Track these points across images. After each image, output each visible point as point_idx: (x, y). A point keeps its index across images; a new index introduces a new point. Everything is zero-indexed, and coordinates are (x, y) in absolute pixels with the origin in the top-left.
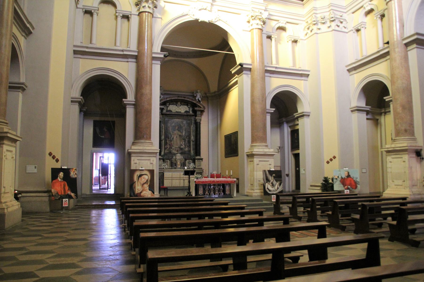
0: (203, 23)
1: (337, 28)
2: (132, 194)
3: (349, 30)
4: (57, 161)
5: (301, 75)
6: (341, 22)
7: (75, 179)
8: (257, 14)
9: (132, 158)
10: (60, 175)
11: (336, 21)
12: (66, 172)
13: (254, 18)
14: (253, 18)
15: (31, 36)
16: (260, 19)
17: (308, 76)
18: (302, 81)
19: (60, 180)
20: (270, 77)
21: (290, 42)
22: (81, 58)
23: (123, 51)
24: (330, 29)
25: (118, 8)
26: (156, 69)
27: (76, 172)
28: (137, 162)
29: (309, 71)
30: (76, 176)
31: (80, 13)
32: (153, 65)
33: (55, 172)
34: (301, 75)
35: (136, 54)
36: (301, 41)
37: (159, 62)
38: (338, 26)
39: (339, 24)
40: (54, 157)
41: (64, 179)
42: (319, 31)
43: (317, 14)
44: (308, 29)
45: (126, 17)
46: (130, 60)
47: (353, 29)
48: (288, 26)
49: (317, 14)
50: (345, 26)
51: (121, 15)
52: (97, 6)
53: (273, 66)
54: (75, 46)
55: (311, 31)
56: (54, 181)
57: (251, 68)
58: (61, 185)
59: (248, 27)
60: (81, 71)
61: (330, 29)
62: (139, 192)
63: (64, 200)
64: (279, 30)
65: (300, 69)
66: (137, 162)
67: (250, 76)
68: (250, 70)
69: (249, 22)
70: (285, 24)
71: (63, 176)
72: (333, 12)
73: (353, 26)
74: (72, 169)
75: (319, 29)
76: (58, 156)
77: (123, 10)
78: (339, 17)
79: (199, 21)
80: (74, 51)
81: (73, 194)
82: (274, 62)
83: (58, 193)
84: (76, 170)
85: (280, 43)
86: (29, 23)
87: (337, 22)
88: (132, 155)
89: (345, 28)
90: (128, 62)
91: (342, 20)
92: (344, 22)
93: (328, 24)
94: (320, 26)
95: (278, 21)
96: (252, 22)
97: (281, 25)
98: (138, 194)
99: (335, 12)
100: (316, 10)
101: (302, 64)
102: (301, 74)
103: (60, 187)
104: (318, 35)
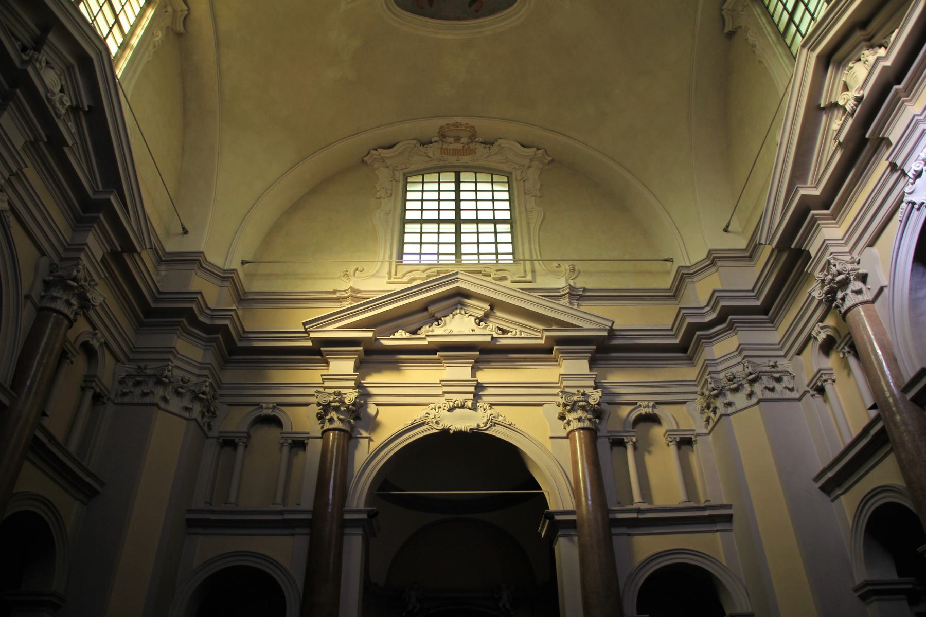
0: (460, 434)
1: (769, 395)
3: (801, 392)
5: (712, 520)
6: (779, 380)
8: (576, 398)
11: (765, 378)
13: (573, 407)
14: (568, 408)
16: (583, 408)
17: (728, 518)
18: (718, 533)
20: (629, 535)
21: (673, 448)
22: (200, 534)
23: (281, 512)
24: (754, 400)
25: (286, 429)
26: (354, 545)
29: (729, 506)
32: (345, 538)
34: (712, 520)
35: (309, 516)
36: (698, 438)
37: (360, 531)
38: (772, 390)
39: (772, 384)
42: (730, 410)
43: (718, 372)
44: (708, 407)
45: (299, 444)
46: (298, 530)
47: (808, 389)
48: (661, 411)
49: (718, 372)
50: (790, 386)
51: (290, 441)
52: (245, 430)
53: (635, 506)
54: (190, 511)
55: (715, 413)
57: (575, 521)
59: (560, 429)
61: (754, 400)
64: (641, 426)
65: (707, 504)
67: (576, 539)
68: (572, 524)
69: (562, 417)
70: (654, 407)
72: (748, 362)
73: (806, 382)
75: (729, 404)
77: (294, 430)
78: (768, 369)
79: (451, 432)
82: (637, 497)
85: (650, 452)
86: (90, 474)
87: (766, 381)
89: (791, 390)
90: (293, 535)
91: (777, 375)
92: (785, 378)
93: (747, 389)
94: (730, 397)
95: (636, 403)
96: (570, 416)
97: (643, 411)
99: (750, 359)
100: (715, 365)
101: (713, 492)
102: (710, 516)
104: (731, 417)
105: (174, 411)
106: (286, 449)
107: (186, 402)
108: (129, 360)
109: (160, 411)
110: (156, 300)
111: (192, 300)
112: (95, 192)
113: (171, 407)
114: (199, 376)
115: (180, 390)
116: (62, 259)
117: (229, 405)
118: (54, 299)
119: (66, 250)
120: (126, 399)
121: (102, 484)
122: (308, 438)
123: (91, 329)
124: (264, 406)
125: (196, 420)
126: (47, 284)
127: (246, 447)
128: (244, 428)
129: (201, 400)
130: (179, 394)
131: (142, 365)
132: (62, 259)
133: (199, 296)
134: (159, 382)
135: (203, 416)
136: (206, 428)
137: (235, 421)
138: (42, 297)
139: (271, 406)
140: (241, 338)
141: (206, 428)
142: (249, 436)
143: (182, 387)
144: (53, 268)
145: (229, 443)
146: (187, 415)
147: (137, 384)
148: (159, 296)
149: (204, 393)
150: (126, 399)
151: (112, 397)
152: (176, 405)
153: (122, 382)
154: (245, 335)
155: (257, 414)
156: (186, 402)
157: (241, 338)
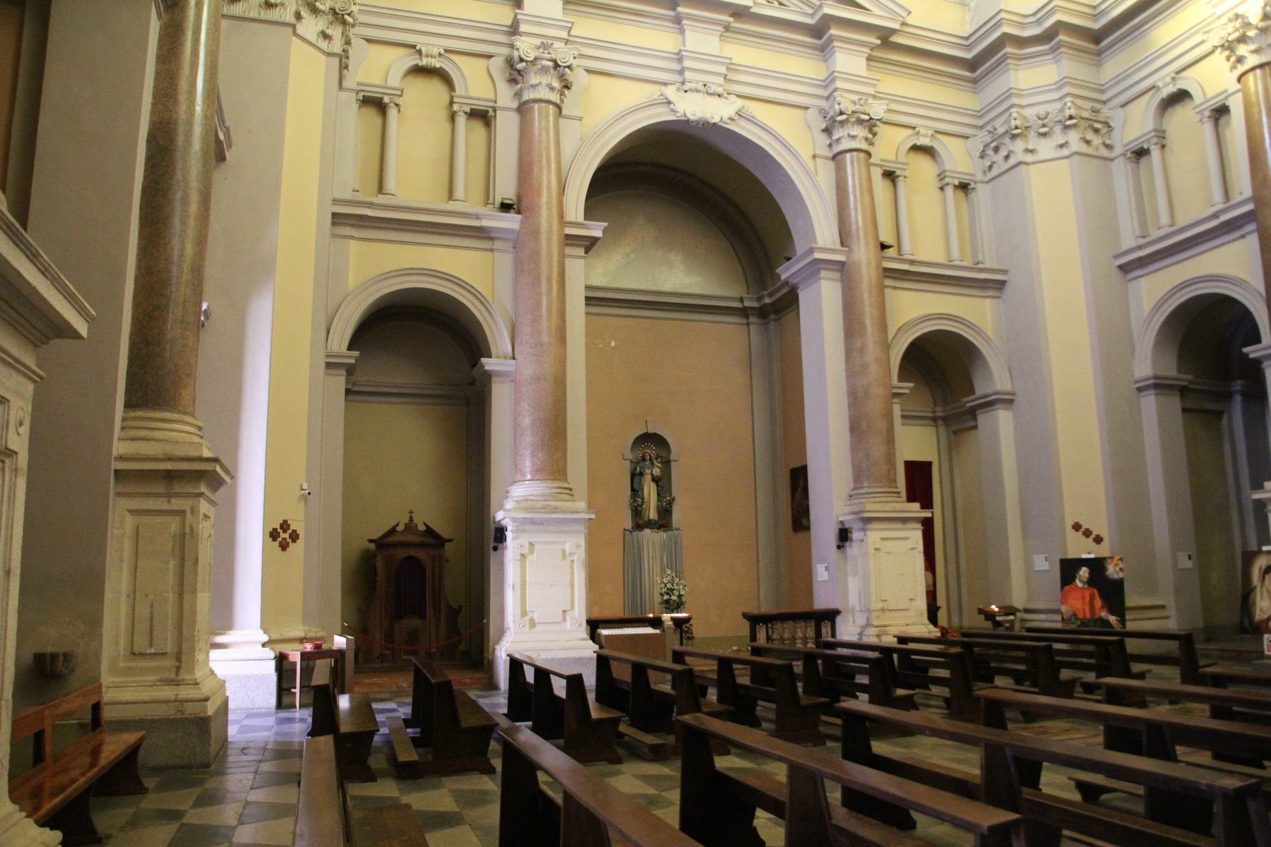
2: (1247, 623)
4: (1098, 540)
7: (1120, 583)
12: (1097, 566)
15: (1008, 287)
19: (1080, 585)
23: (1215, 216)
25: (1198, 97)
27: (1121, 565)
30: (1121, 575)
31: (1121, 170)
33: (1069, 568)
35: (1250, 207)
40: (1087, 533)
41: (1091, 582)
45: (1221, 112)
51: (1207, 113)
56: (1067, 588)
58: (1083, 598)
60: (1147, 308)
62: (1265, 616)
76: (1100, 528)
77: (1209, 95)
80: (1121, 267)
81: (1112, 619)
83: (1075, 615)
84: (1121, 559)
90: (1243, 236)
98: (1261, 622)
103: (1083, 601)
105: (1048, 157)
106: (1208, 127)
107: (1059, 137)
108: (981, 128)
109: (1031, 167)
110: (968, 48)
111: (998, 24)
112: (812, 15)
113: (1042, 155)
114: (1060, 99)
115: (1043, 130)
116: (827, 98)
117: (1122, 106)
118: (838, 140)
119: (825, 87)
120: (995, 172)
121: (1005, 272)
122: (1227, 98)
123: (910, 132)
124: (1160, 84)
126: (827, 131)
127: (1163, 146)
128: (1150, 126)
129: (1074, 126)
130: (1044, 135)
131: (990, 128)
132: (827, 98)
133: (1003, 15)
134: (1014, 137)
135: (1088, 142)
136: (1104, 152)
137: (1136, 123)
138: (830, 146)
139: (1168, 79)
140: (1095, 17)
141: (1104, 152)
142: (1161, 135)
143: (1044, 126)
144: (823, 113)
145: (1141, 153)
146: (1065, 152)
147: (996, 149)
148: (966, 42)
149: (1071, 117)
150: (995, 172)
151: (979, 177)
152: (1046, 148)
153: (982, 157)
154: (1098, 10)
156: (1059, 137)
157: (1095, 17)
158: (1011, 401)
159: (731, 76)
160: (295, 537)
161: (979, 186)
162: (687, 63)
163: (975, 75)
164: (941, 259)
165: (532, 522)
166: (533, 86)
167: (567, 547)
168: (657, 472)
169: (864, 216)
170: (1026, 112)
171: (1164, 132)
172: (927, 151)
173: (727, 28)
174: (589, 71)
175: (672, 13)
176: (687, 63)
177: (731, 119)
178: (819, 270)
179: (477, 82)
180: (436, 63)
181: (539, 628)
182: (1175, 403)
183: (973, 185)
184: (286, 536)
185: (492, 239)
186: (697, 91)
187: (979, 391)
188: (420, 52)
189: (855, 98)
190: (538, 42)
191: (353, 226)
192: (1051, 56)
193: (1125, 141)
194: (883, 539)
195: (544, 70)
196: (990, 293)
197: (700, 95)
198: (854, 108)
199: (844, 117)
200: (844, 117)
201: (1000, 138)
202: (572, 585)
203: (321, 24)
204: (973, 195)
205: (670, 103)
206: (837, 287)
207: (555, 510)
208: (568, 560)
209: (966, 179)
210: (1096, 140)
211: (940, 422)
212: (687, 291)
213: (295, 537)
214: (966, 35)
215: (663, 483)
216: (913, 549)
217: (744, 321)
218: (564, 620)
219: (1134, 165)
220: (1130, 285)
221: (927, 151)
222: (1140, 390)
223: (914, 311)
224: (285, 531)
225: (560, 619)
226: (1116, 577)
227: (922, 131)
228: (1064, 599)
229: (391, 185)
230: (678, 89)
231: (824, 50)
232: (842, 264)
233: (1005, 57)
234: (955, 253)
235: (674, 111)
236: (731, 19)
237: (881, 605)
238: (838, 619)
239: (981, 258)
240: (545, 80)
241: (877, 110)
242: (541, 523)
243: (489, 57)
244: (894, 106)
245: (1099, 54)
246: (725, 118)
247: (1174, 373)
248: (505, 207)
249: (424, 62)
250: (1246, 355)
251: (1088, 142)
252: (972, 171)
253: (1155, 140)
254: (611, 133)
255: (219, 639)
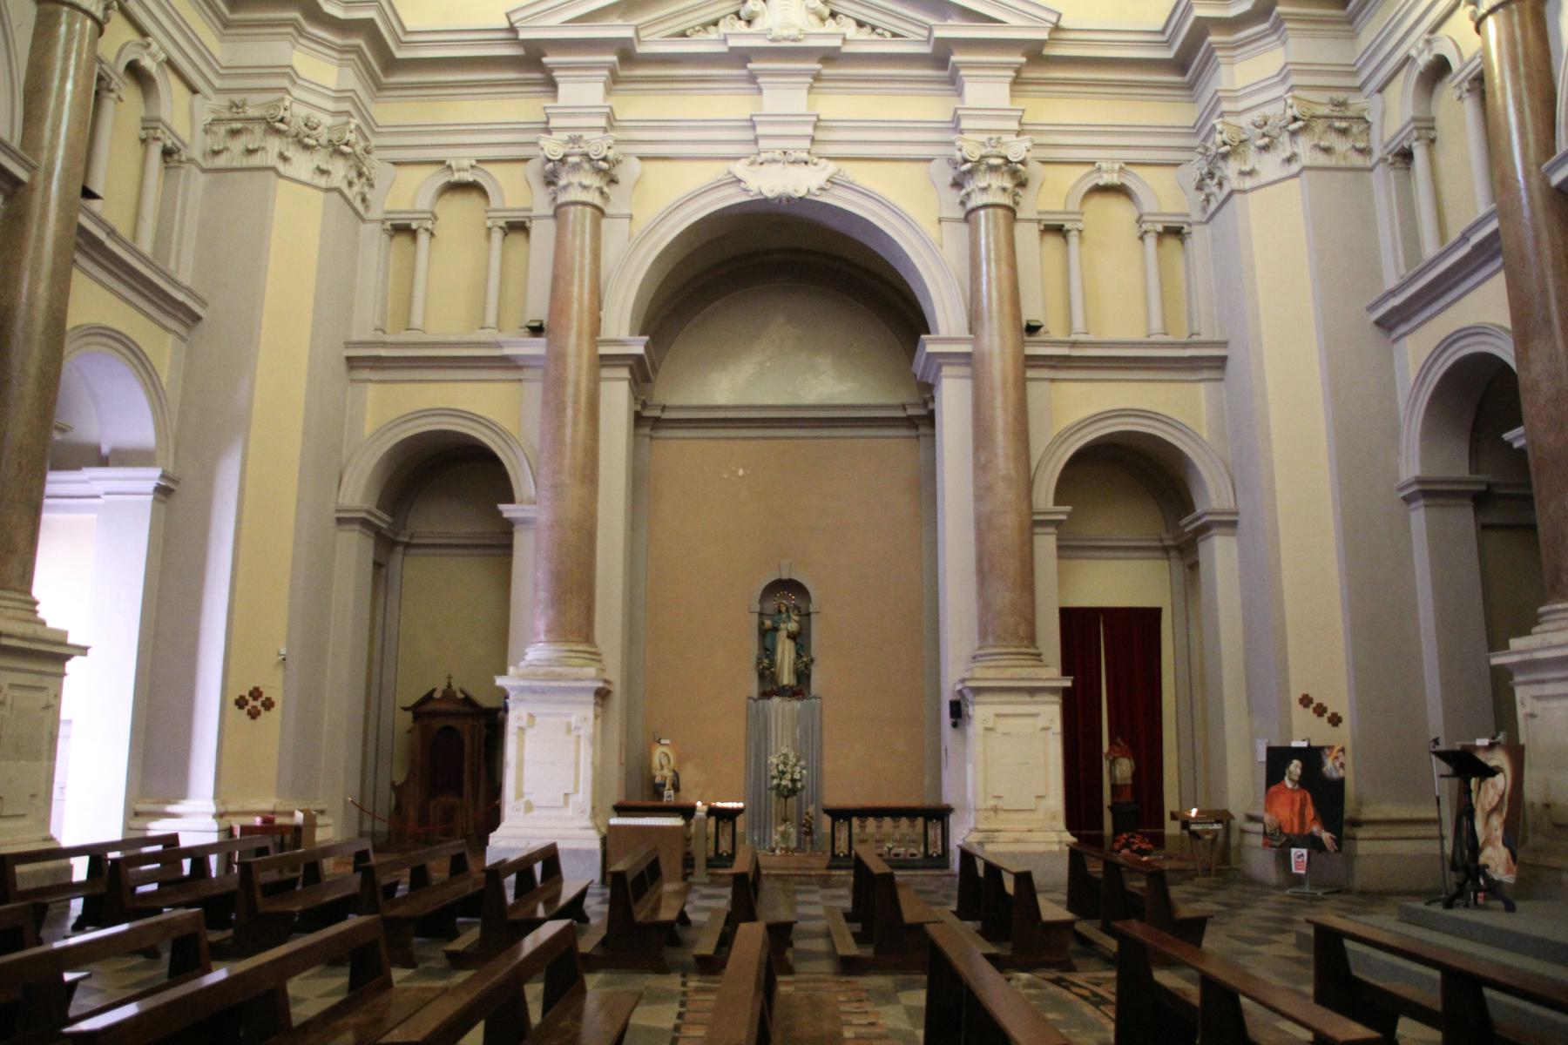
4: (1335, 720)
7: (1340, 783)
9: (1520, 693)
10: (1292, 767)
12: (1312, 757)
15: (1230, 363)
19: (1289, 785)
28: (1537, 707)
31: (1382, 183)
33: (1278, 758)
40: (1320, 710)
51: (1466, 85)
56: (1273, 789)
58: (1292, 803)
63: (1294, 851)
66: (1537, 707)
71: (1299, 771)
74: (1331, 748)
76: (1339, 703)
80: (1378, 323)
81: (1326, 836)
88: (1518, 679)
105: (1272, 178)
107: (1285, 147)
109: (1250, 196)
110: (1168, 44)
121: (1224, 344)
124: (1413, 53)
125: (1304, 168)
127: (1433, 141)
130: (1265, 148)
135: (1327, 150)
136: (1359, 161)
139: (1421, 44)
141: (1359, 161)
146: (1295, 168)
148: (1164, 34)
151: (1196, 216)
152: (1270, 166)
153: (1199, 188)
155: (1415, 75)
158: (1233, 524)
159: (819, 135)
160: (268, 705)
161: (1195, 229)
162: (760, 130)
163: (1186, 79)
164: (1138, 335)
165: (533, 691)
166: (565, 187)
167: (573, 720)
168: (793, 626)
169: (999, 291)
170: (1244, 121)
171: (1433, 120)
172: (1120, 190)
173: (817, 77)
174: (642, 158)
175: (744, 72)
176: (760, 130)
177: (822, 189)
178: (939, 367)
179: (514, 190)
180: (468, 177)
181: (535, 813)
182: (1463, 519)
183: (1186, 229)
184: (258, 704)
185: (520, 368)
186: (774, 161)
187: (1199, 510)
188: (449, 167)
189: (984, 137)
190: (565, 136)
191: (372, 368)
192: (1275, 37)
193: (1387, 138)
194: (998, 716)
195: (576, 167)
196: (1206, 374)
197: (779, 166)
198: (984, 152)
199: (968, 166)
200: (968, 166)
201: (1214, 163)
202: (577, 764)
203: (320, 159)
204: (1188, 241)
205: (740, 181)
206: (967, 386)
207: (559, 677)
208: (574, 734)
209: (1175, 221)
210: (1341, 145)
211: (1173, 554)
212: (838, 402)
213: (268, 705)
214: (1159, 27)
215: (800, 639)
216: (1046, 729)
217: (913, 433)
218: (566, 804)
219: (1401, 173)
220: (1396, 347)
221: (1120, 190)
222: (1408, 500)
223: (1075, 410)
224: (255, 699)
225: (561, 803)
226: (1335, 775)
227: (1104, 165)
228: (1269, 802)
229: (417, 320)
230: (752, 163)
231: (954, 82)
232: (968, 355)
233: (1211, 51)
234: (1156, 324)
235: (746, 190)
236: (819, 66)
237: (992, 803)
238: (952, 818)
239: (1196, 328)
240: (576, 178)
241: (1017, 149)
242: (543, 691)
243: (526, 160)
244: (1039, 140)
245: (1350, 21)
246: (813, 189)
247: (1461, 470)
248: (537, 330)
249: (456, 177)
250: (1509, 444)
251: (1327, 150)
252: (1186, 210)
253: (1415, 134)
254: (663, 230)
255: (171, 809)
